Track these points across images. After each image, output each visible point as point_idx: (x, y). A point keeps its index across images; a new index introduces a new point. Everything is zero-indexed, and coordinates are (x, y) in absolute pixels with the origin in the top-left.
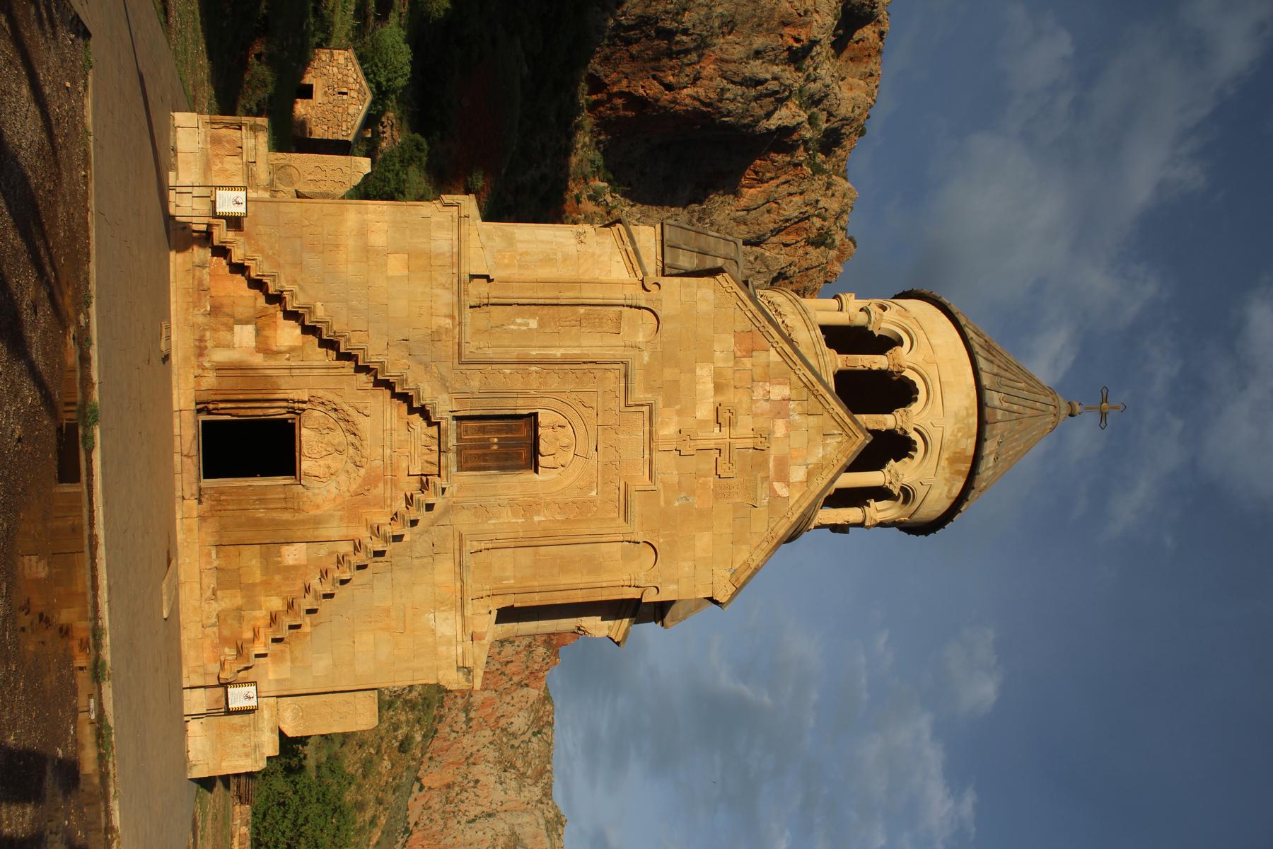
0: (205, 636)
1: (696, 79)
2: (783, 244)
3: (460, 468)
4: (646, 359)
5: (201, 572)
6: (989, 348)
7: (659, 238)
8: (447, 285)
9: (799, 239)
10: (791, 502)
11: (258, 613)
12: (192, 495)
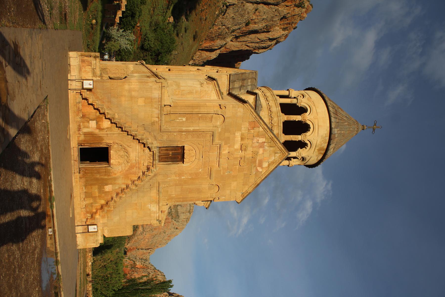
0: (82, 211)
2: (286, 5)
3: (160, 161)
4: (220, 130)
5: (80, 193)
6: (336, 113)
7: (228, 79)
8: (157, 108)
9: (292, 4)
10: (262, 173)
11: (97, 205)
12: (77, 172)
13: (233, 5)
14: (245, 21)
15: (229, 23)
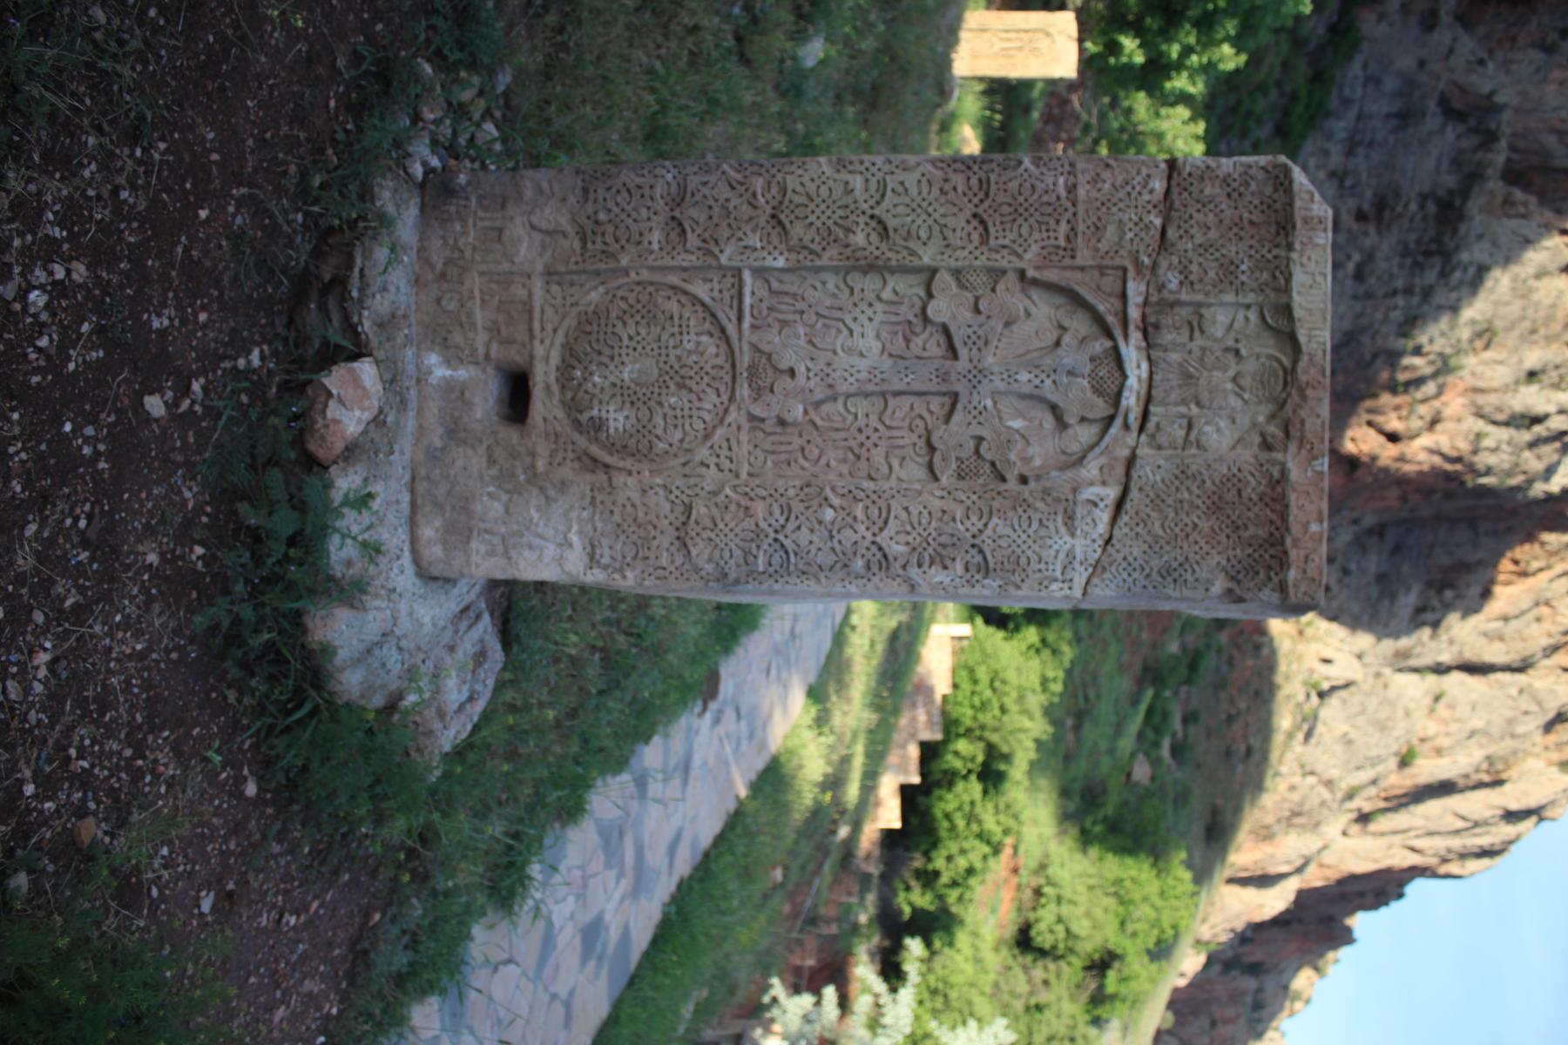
1: (1434, 422)
13: (1347, 686)
14: (1395, 748)
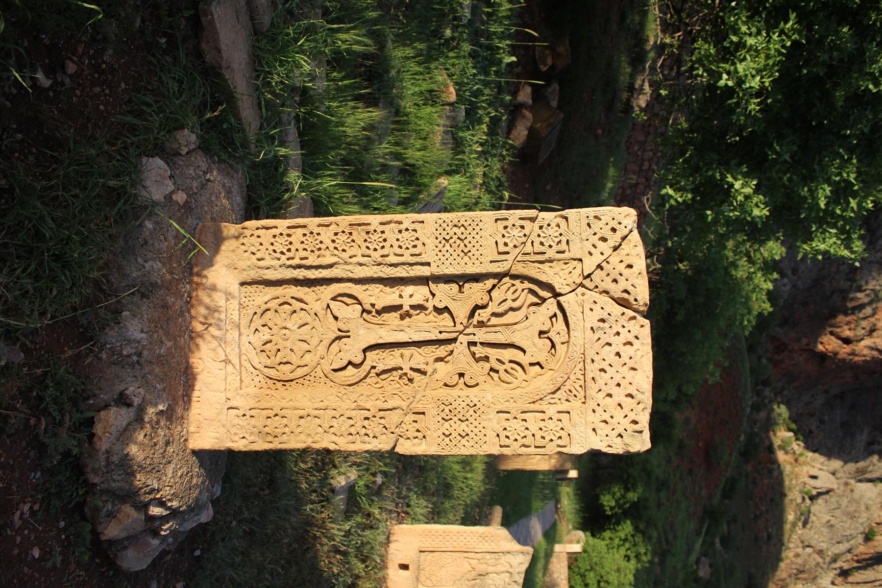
1: (872, 331)
14: (861, 529)
15: (821, 539)
